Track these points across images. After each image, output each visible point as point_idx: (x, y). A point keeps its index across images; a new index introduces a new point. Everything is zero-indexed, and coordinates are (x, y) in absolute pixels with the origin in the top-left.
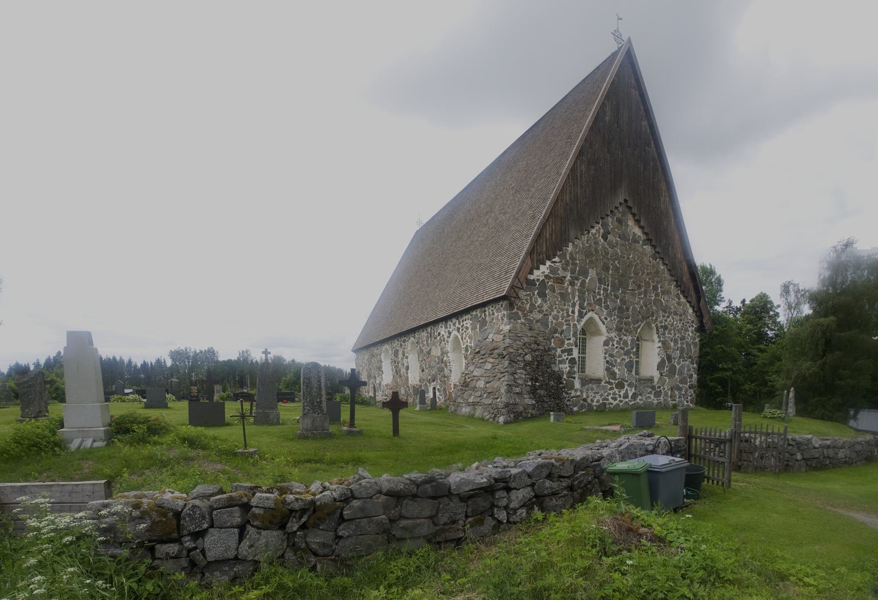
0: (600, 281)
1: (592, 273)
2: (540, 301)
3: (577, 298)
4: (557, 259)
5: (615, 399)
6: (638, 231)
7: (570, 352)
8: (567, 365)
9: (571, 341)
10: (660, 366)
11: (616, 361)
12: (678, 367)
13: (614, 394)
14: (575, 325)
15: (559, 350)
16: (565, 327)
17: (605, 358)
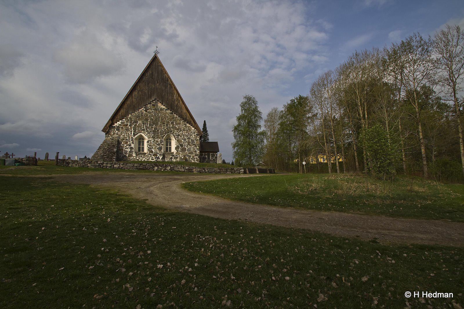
0: (144, 124)
1: (140, 122)
2: (117, 132)
3: (132, 130)
4: (124, 120)
6: (163, 107)
7: (130, 145)
8: (129, 149)
10: (177, 148)
11: (152, 147)
13: (152, 158)
14: (132, 138)
16: (128, 138)
17: (148, 146)
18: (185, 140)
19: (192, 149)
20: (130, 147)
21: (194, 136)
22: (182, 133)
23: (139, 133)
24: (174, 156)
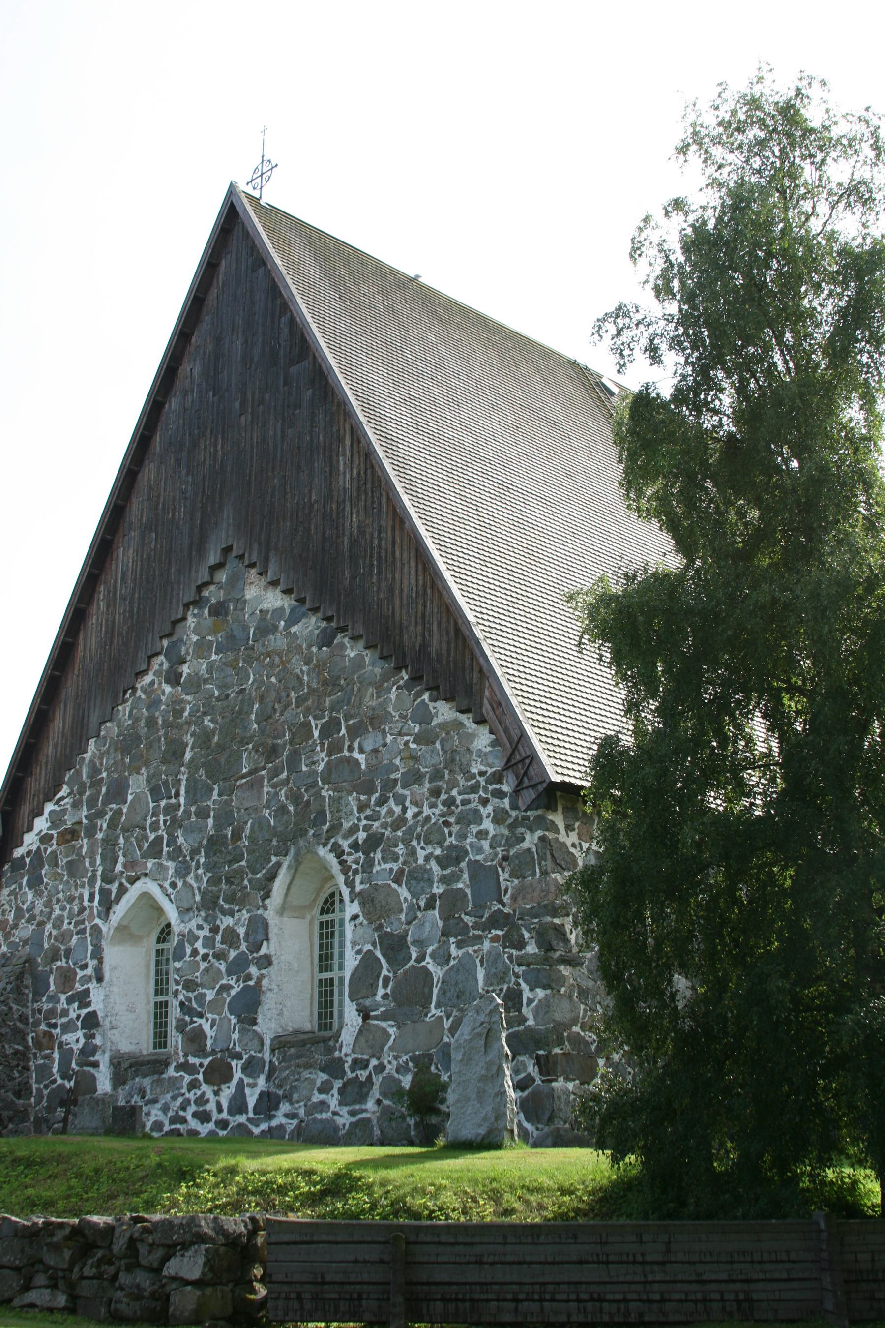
1: (138, 784)
2: (30, 896)
5: (204, 1117)
8: (80, 1034)
9: (89, 971)
11: (201, 998)
12: (437, 972)
14: (96, 929)
15: (63, 998)
18: (416, 877)
19: (481, 974)
20: (84, 1012)
21: (499, 817)
22: (398, 809)
23: (133, 881)
24: (334, 1068)
